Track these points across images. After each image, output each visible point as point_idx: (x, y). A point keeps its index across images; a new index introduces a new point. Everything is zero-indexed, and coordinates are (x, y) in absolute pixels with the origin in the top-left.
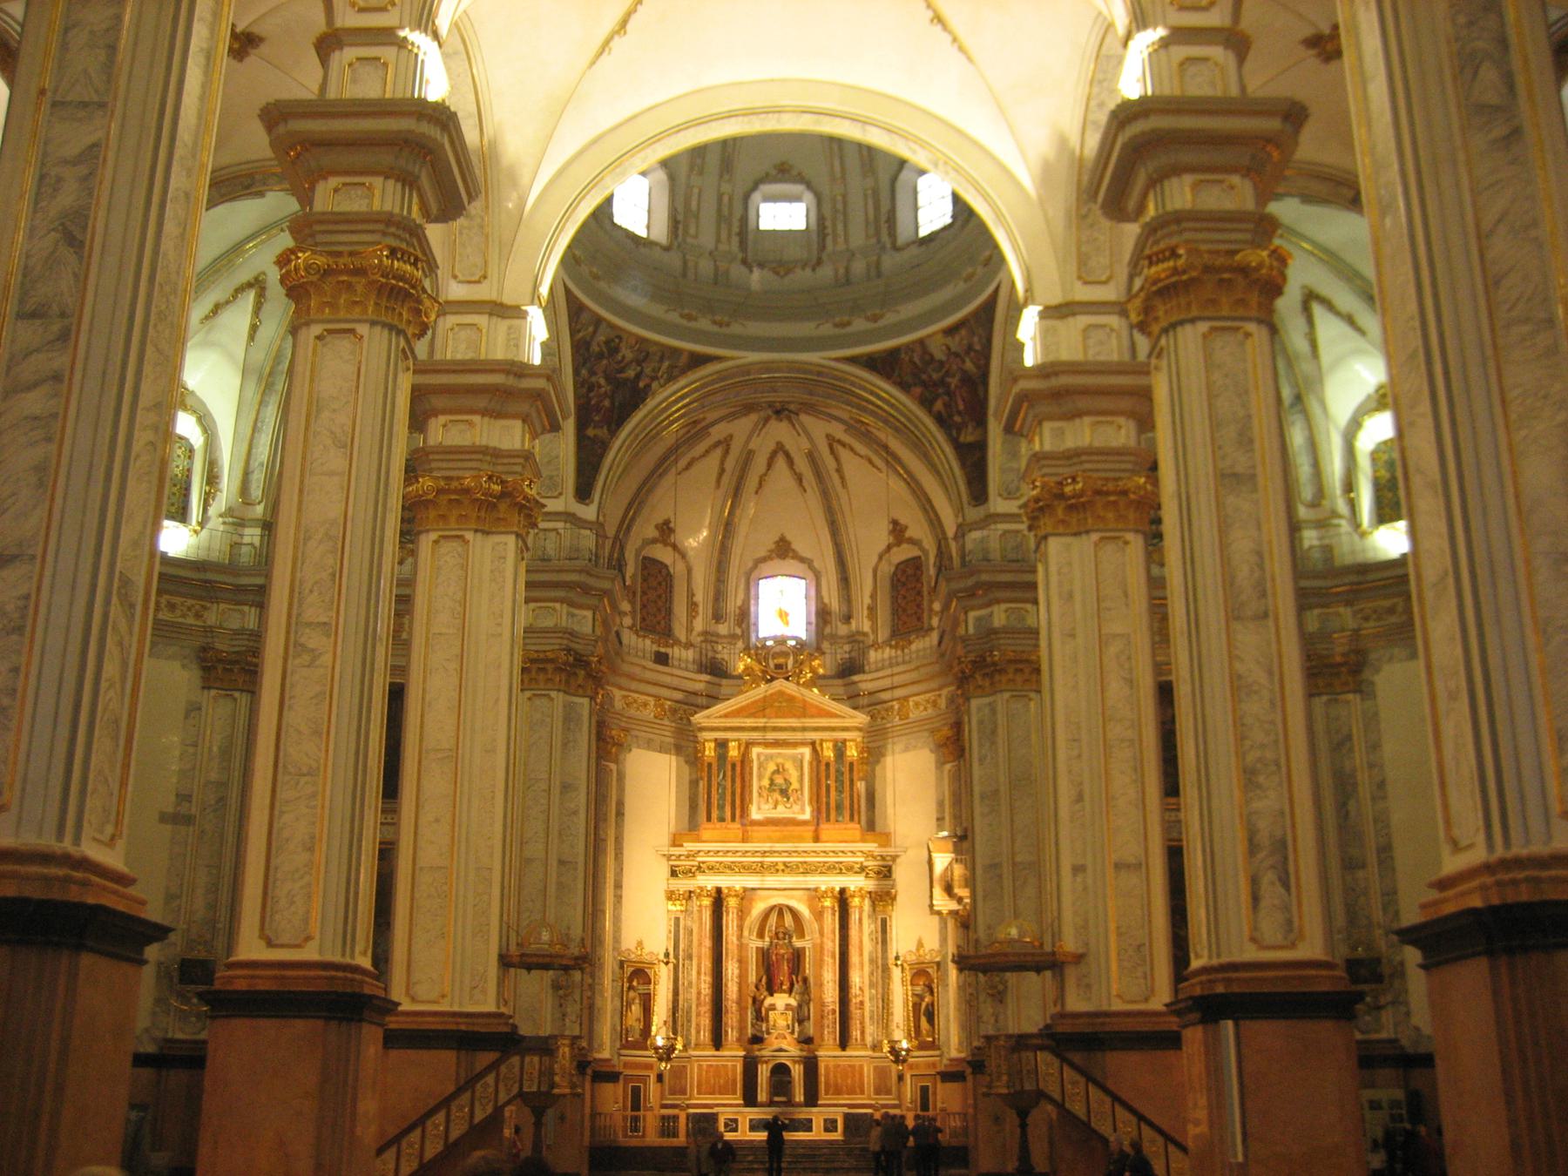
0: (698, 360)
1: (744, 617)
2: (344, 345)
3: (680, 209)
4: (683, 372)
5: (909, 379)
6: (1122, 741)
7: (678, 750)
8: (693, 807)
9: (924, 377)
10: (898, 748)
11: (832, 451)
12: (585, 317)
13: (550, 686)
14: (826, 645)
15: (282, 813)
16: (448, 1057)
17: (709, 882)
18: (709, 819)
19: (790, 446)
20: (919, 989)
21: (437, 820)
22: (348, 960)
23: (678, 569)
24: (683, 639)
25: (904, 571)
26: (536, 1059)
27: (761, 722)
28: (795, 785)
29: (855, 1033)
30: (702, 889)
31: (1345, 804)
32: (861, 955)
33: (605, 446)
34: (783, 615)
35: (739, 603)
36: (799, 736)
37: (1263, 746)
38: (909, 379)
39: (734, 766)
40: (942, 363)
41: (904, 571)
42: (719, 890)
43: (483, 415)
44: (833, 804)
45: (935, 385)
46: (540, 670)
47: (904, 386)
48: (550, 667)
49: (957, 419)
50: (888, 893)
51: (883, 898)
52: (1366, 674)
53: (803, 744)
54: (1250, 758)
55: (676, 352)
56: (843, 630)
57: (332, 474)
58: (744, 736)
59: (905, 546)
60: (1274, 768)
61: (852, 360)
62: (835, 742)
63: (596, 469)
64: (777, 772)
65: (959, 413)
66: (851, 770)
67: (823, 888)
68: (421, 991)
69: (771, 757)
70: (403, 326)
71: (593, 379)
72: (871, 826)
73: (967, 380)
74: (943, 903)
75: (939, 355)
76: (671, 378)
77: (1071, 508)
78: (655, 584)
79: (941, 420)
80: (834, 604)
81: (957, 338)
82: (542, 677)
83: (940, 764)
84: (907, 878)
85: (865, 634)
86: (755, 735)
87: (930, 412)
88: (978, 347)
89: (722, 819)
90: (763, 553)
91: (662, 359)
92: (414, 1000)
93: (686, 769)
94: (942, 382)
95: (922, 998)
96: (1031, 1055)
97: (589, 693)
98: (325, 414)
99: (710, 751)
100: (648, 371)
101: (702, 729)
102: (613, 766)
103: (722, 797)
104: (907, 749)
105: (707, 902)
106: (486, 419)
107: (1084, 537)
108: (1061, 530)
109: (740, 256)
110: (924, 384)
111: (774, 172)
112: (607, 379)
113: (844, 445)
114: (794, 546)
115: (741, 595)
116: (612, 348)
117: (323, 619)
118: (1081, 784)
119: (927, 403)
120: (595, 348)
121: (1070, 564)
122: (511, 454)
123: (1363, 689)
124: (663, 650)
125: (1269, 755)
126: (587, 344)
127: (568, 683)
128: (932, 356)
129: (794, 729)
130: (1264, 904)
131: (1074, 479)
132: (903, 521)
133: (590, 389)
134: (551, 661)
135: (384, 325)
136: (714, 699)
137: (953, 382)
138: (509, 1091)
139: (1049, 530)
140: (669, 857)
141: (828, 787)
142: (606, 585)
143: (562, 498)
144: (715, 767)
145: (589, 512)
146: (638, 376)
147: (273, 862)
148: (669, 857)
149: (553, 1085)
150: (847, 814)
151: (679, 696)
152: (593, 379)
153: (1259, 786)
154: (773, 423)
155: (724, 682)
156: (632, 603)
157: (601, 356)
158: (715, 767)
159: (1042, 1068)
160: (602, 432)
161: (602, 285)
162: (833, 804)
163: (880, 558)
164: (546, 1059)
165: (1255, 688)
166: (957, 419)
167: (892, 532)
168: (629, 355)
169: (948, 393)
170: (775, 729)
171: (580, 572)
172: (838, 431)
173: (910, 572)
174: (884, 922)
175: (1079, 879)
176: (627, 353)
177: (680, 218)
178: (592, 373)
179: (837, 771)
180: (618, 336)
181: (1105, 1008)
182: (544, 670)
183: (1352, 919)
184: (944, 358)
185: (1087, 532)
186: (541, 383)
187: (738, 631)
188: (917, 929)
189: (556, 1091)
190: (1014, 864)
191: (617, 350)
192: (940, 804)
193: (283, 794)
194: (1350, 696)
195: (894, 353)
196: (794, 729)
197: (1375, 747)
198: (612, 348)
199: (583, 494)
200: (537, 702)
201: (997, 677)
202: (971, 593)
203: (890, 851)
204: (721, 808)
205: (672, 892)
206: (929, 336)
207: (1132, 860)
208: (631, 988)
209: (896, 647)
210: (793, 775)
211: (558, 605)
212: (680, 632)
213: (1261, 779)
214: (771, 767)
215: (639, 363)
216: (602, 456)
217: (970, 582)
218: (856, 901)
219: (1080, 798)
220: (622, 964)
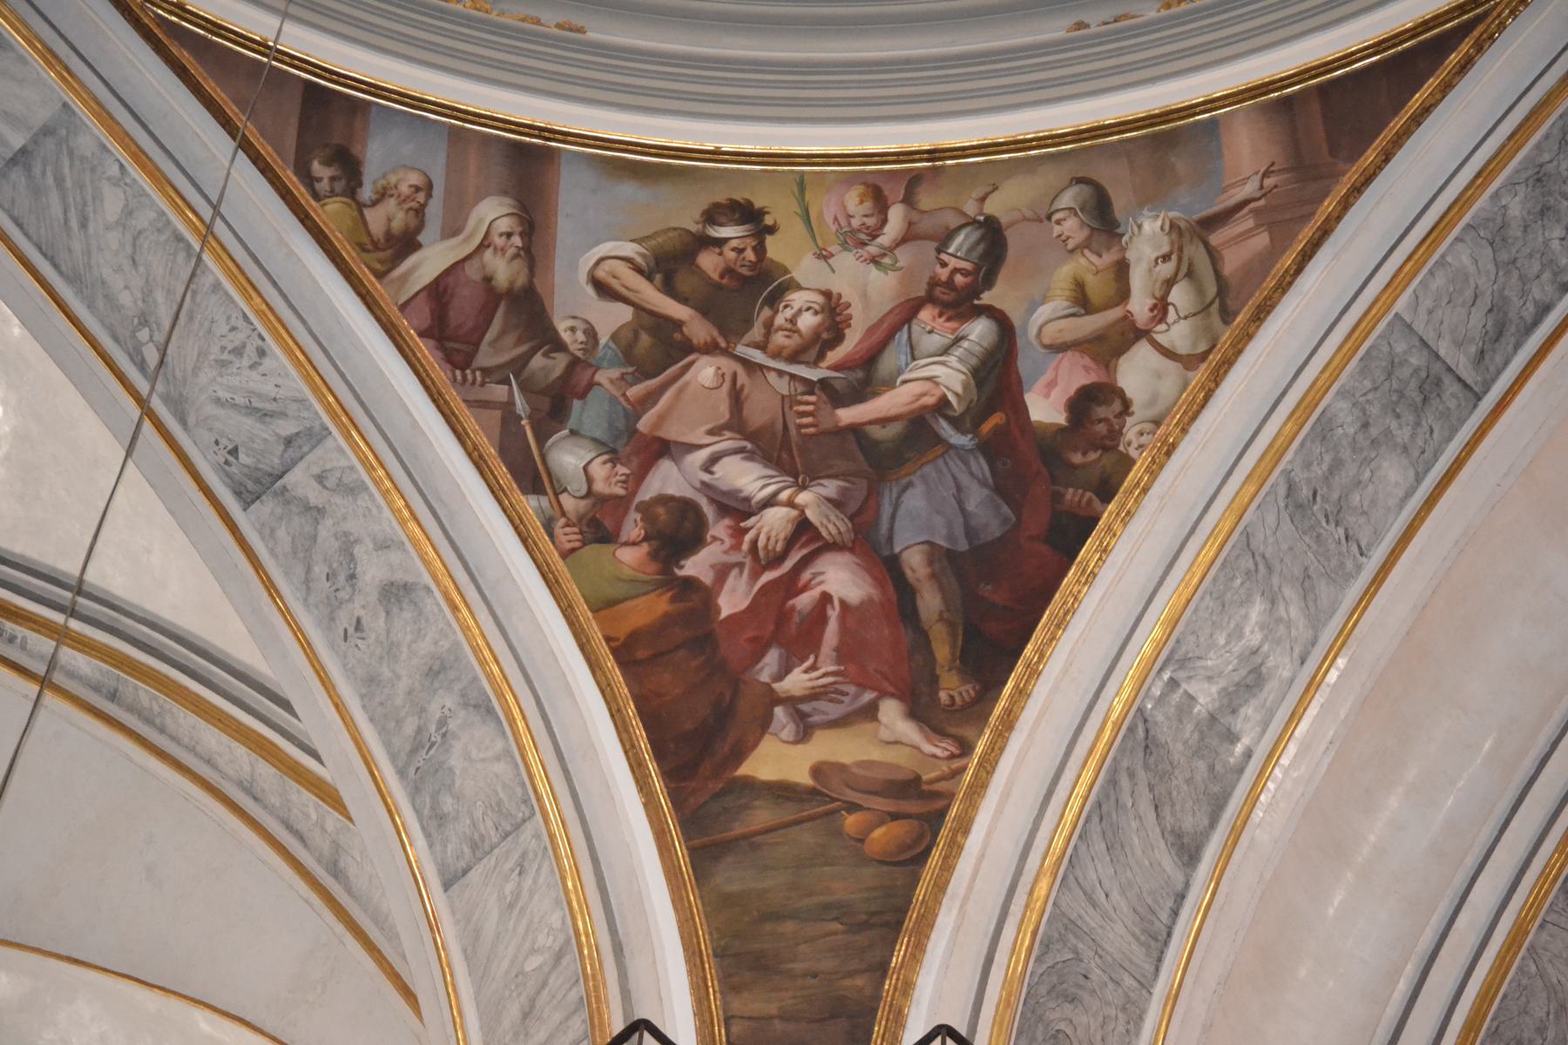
55: (1168, 140)
71: (667, 480)
76: (1236, 307)
91: (1103, 220)
100: (1043, 314)
112: (770, 447)
120: (575, 308)
126: (528, 308)
133: (677, 531)
146: (998, 376)
152: (667, 480)
160: (894, 737)
168: (867, 288)
191: (762, 283)
215: (960, 302)
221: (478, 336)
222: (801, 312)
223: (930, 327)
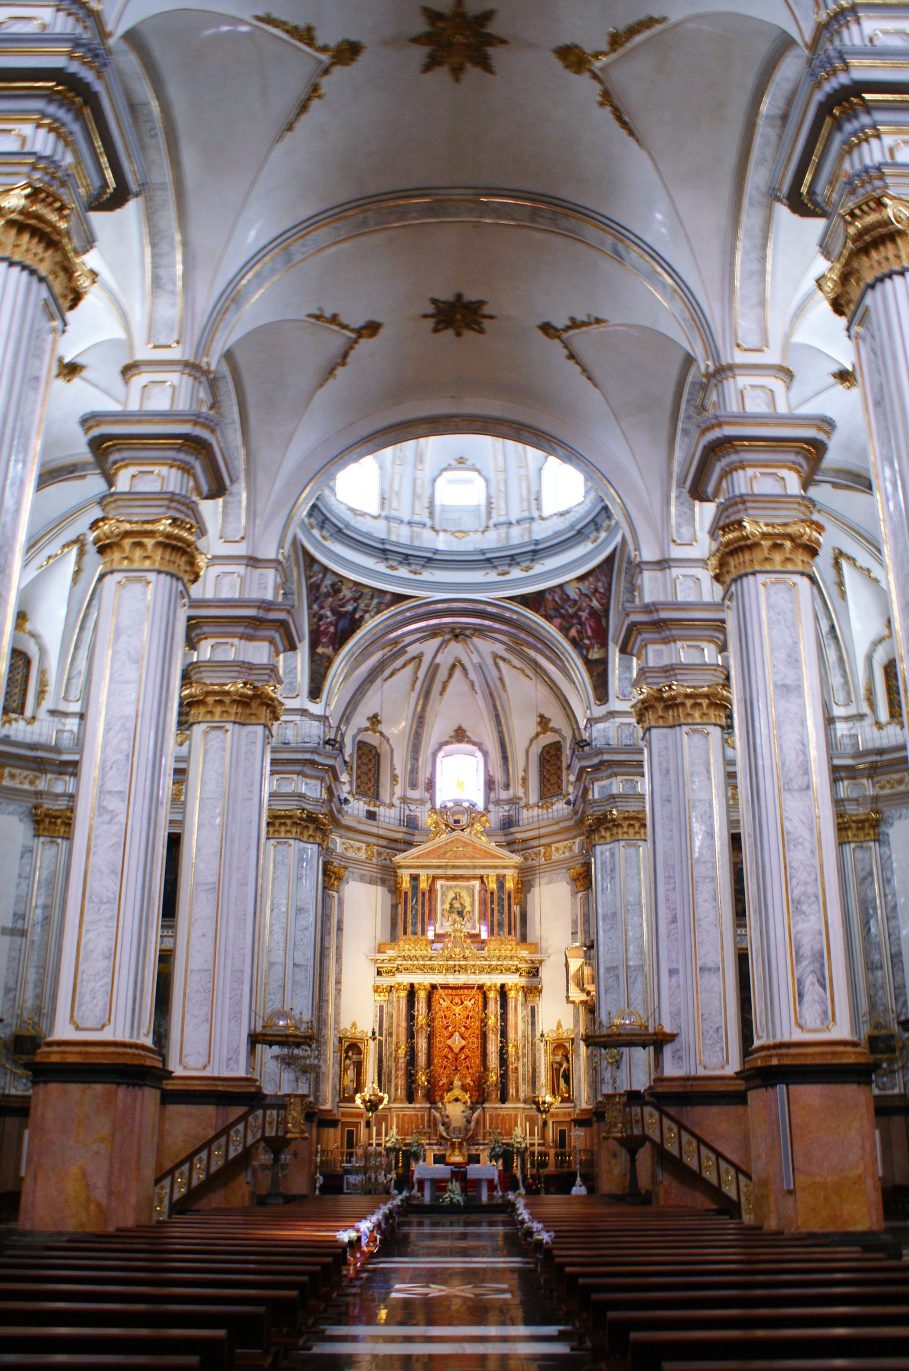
0: (399, 598)
1: (430, 785)
2: (137, 588)
3: (387, 490)
4: (388, 606)
5: (552, 613)
6: (705, 878)
7: (383, 882)
8: (394, 925)
9: (563, 611)
10: (543, 881)
11: (496, 664)
12: (316, 568)
13: (289, 835)
14: (491, 807)
15: (88, 931)
16: (211, 1109)
17: (405, 979)
18: (405, 933)
19: (465, 661)
20: (558, 1058)
21: (203, 935)
22: (135, 1040)
23: (384, 750)
24: (388, 801)
25: (548, 752)
26: (275, 1112)
27: (443, 862)
28: (468, 908)
29: (512, 1091)
30: (399, 984)
31: (868, 922)
32: (516, 1033)
33: (330, 661)
34: (460, 784)
35: (428, 775)
36: (471, 872)
37: (806, 883)
38: (552, 613)
39: (423, 894)
40: (575, 602)
41: (548, 752)
42: (412, 985)
43: (241, 638)
44: (496, 922)
45: (571, 617)
46: (281, 824)
47: (548, 618)
48: (289, 822)
49: (587, 642)
50: (536, 988)
51: (532, 991)
52: (883, 828)
53: (474, 878)
54: (796, 893)
56: (504, 795)
57: (128, 682)
58: (432, 872)
59: (549, 733)
60: (813, 899)
61: (511, 598)
62: (498, 876)
63: (324, 676)
64: (455, 898)
65: (588, 638)
66: (509, 897)
67: (488, 984)
68: (191, 1061)
69: (451, 887)
70: (181, 575)
71: (322, 612)
72: (524, 938)
73: (593, 613)
74: (577, 996)
75: (573, 595)
77: (667, 708)
78: (366, 761)
79: (574, 643)
80: (499, 776)
81: (587, 583)
82: (283, 829)
83: (574, 893)
84: (551, 976)
85: (520, 799)
86: (439, 872)
87: (567, 636)
88: (601, 590)
89: (415, 933)
90: (446, 739)
91: (372, 598)
92: (185, 1068)
93: (388, 896)
94: (576, 615)
95: (561, 1065)
96: (639, 1109)
97: (318, 840)
98: (124, 639)
99: (406, 885)
100: (362, 606)
101: (400, 867)
102: (335, 894)
103: (415, 917)
104: (550, 882)
105: (403, 994)
106: (243, 642)
107: (678, 728)
108: (661, 722)
109: (429, 523)
110: (562, 617)
111: (454, 463)
112: (333, 611)
113: (504, 660)
114: (468, 734)
115: (429, 769)
116: (336, 589)
117: (119, 788)
118: (675, 909)
119: (565, 630)
120: (324, 590)
121: (667, 748)
122: (262, 667)
123: (881, 840)
124: (372, 809)
125: (810, 890)
127: (302, 833)
128: (568, 596)
129: (467, 867)
130: (807, 998)
131: (670, 687)
132: (547, 716)
134: (290, 817)
135: (167, 573)
136: (410, 844)
137: (584, 615)
138: (254, 1136)
139: (653, 724)
140: (376, 961)
141: (492, 910)
142: (330, 762)
143: (298, 699)
144: (410, 895)
145: (316, 708)
146: (355, 610)
147: (81, 968)
148: (376, 961)
149: (287, 1131)
150: (506, 930)
151: (383, 842)
152: (322, 612)
153: (803, 913)
154: (453, 644)
155: (417, 832)
156: (350, 775)
157: (327, 595)
158: (410, 895)
159: (647, 1120)
160: (329, 651)
161: (328, 544)
162: (496, 922)
163: (531, 741)
164: (282, 1112)
165: (801, 840)
166: (587, 642)
167: (540, 723)
169: (581, 623)
170: (454, 867)
171: (312, 752)
172: (500, 649)
173: (552, 752)
174: (533, 1009)
175: (674, 979)
176: (346, 593)
177: (386, 496)
178: (322, 607)
179: (499, 898)
180: (342, 579)
181: (693, 1073)
182: (285, 824)
183: (873, 1006)
184: (577, 598)
185: (680, 725)
186: (282, 616)
187: (427, 795)
188: (557, 1014)
189: (289, 1135)
190: (628, 967)
192: (575, 922)
193: (87, 918)
194: (872, 844)
195: (541, 593)
196: (467, 867)
197: (887, 881)
198: (336, 589)
199: (315, 693)
200: (280, 847)
201: (615, 831)
202: (597, 767)
203: (537, 957)
204: (414, 924)
205: (378, 987)
206: (567, 582)
207: (712, 965)
208: (347, 1057)
209: (542, 807)
210: (467, 901)
211: (295, 777)
212: (385, 796)
213: (805, 907)
214: (451, 895)
215: (355, 600)
216: (328, 668)
217: (596, 760)
218: (512, 994)
219: (674, 920)
220: (340, 1040)
221: (313, 589)
222: (341, 595)
223: (351, 602)
